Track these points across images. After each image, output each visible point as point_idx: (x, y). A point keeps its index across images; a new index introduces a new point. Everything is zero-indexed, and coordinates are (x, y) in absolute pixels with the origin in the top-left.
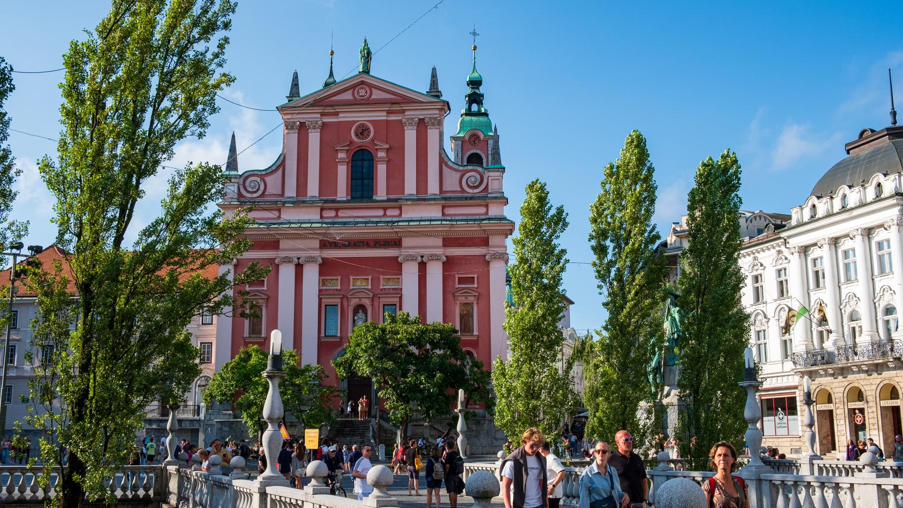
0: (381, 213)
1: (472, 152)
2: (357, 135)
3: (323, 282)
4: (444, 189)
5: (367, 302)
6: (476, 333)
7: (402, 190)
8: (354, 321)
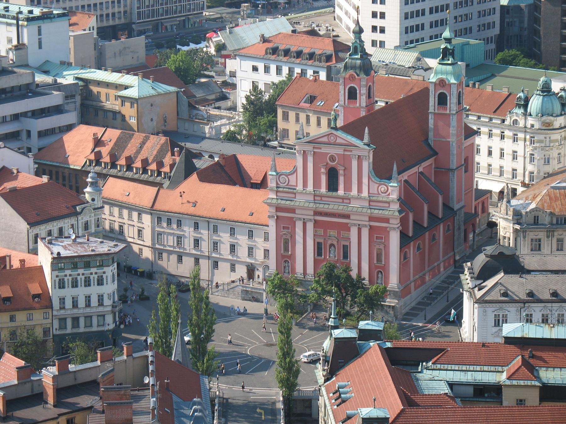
0: (341, 201)
1: (441, 91)
2: (330, 160)
3: (315, 231)
4: (370, 192)
5: (335, 243)
6: (383, 263)
7: (350, 190)
8: (330, 251)
